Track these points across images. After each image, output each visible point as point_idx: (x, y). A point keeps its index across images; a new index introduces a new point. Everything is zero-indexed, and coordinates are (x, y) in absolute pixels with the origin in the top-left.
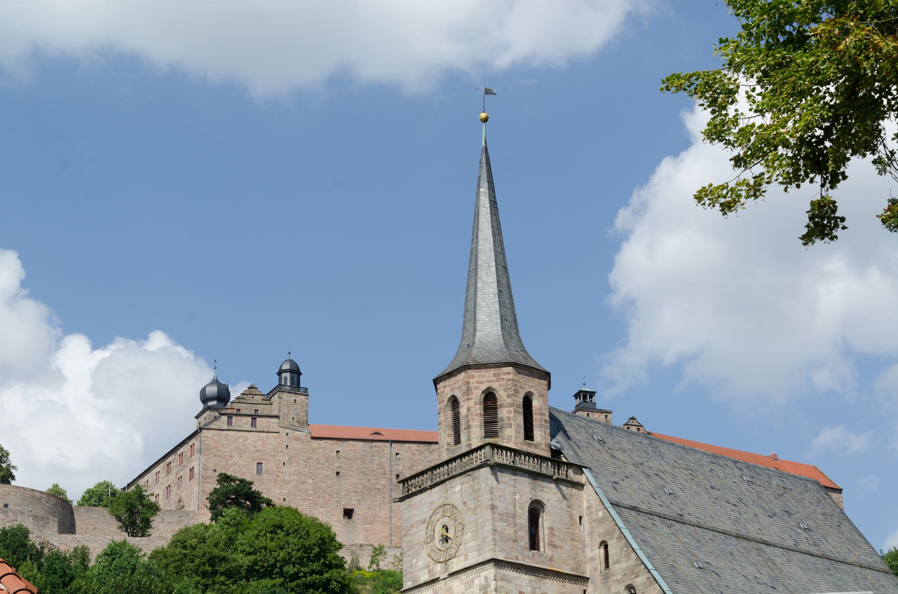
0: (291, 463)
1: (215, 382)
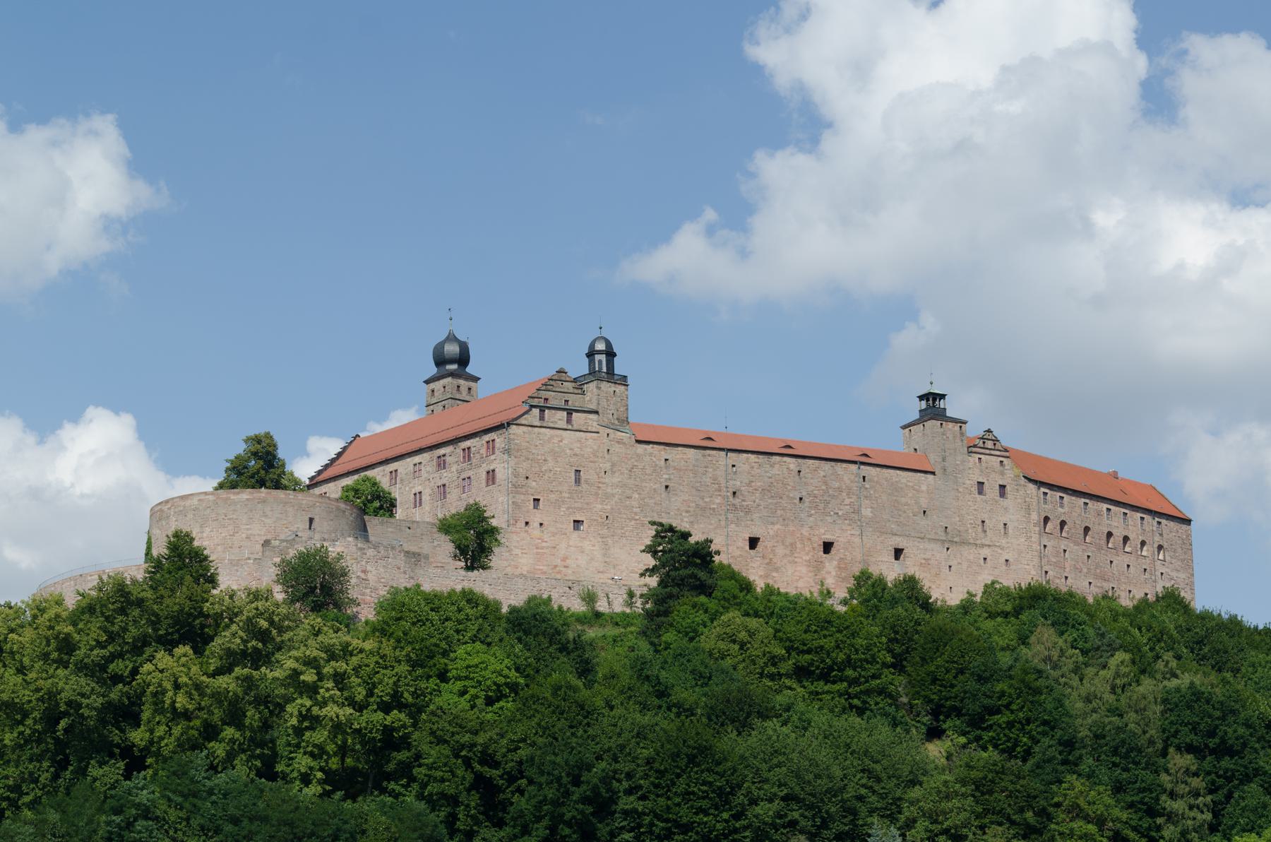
0: (613, 473)
1: (451, 338)
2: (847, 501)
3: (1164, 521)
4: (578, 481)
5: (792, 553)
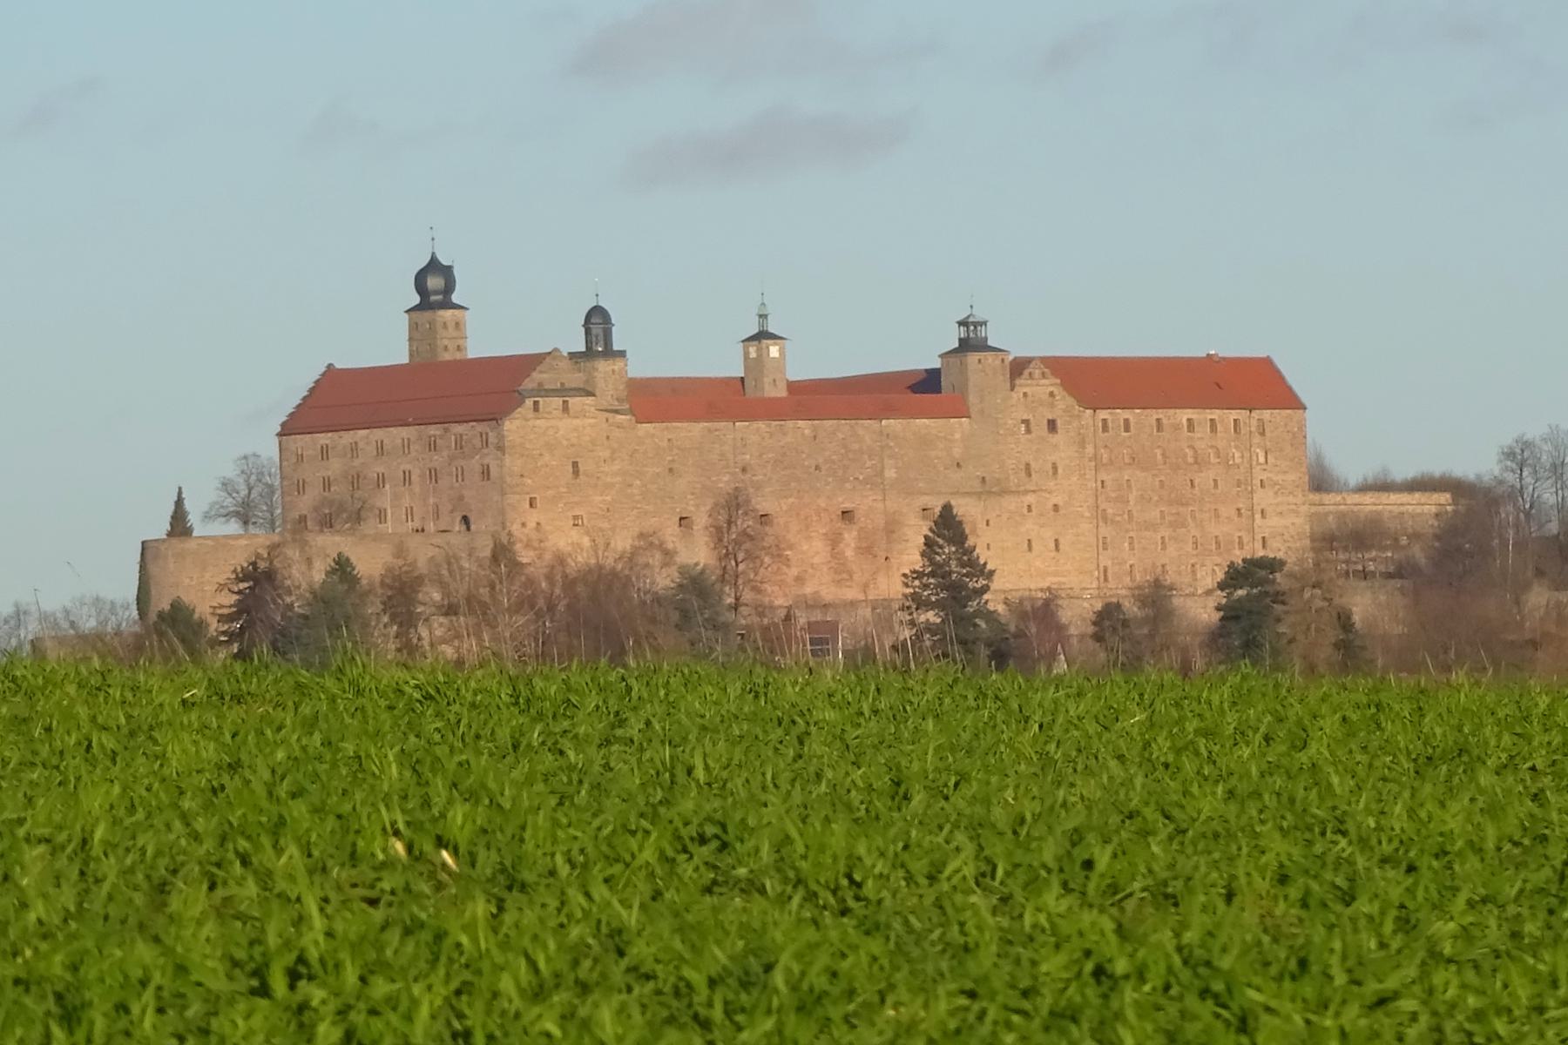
0: (614, 460)
2: (869, 464)
4: (576, 472)
5: (807, 527)
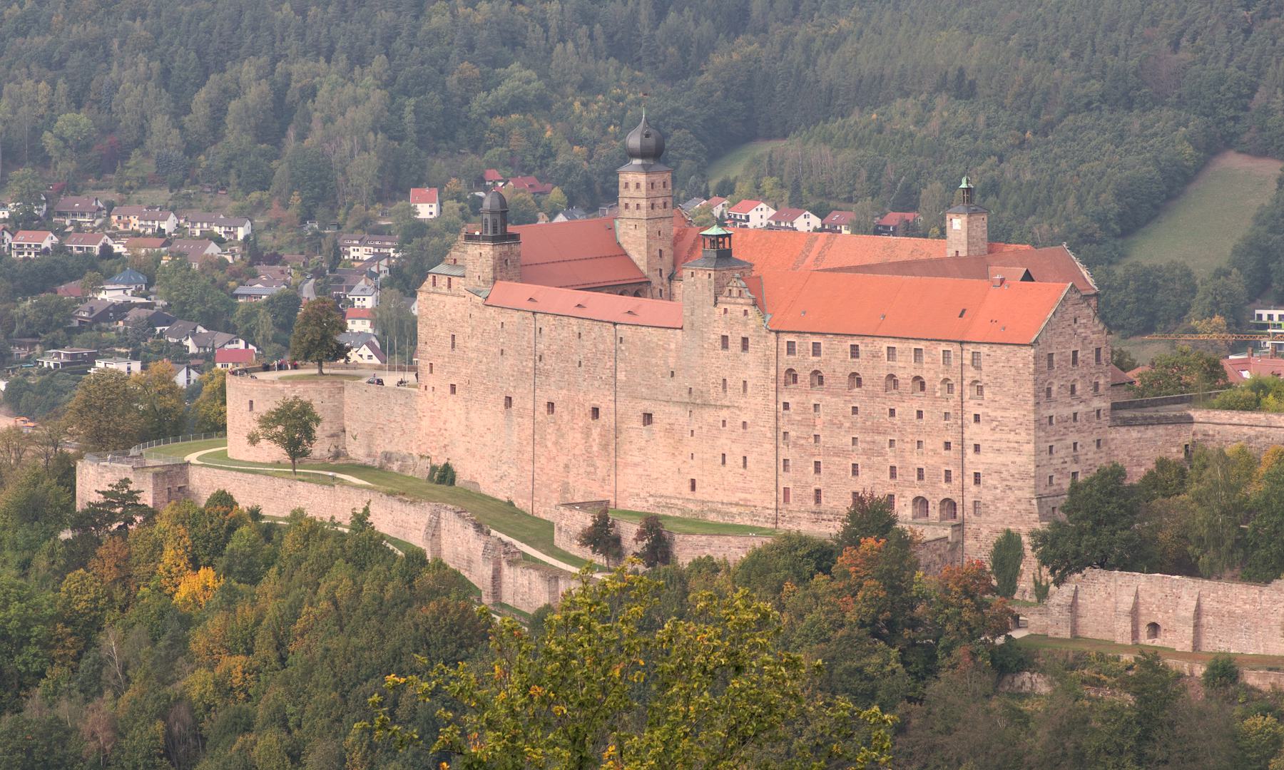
3: (984, 350)
